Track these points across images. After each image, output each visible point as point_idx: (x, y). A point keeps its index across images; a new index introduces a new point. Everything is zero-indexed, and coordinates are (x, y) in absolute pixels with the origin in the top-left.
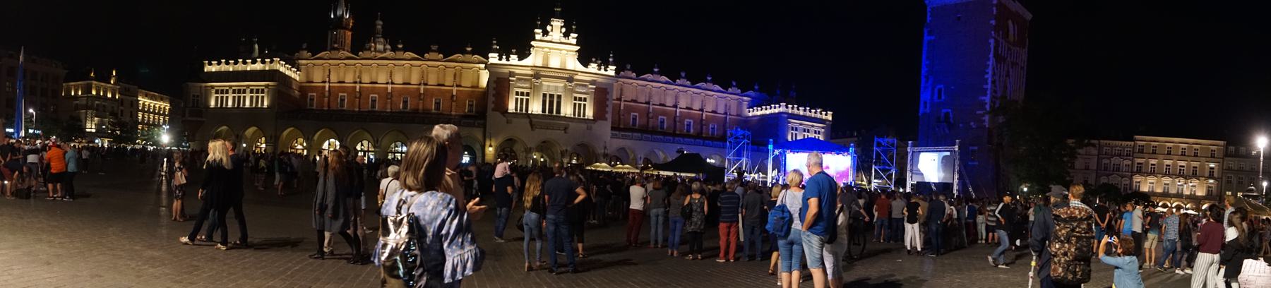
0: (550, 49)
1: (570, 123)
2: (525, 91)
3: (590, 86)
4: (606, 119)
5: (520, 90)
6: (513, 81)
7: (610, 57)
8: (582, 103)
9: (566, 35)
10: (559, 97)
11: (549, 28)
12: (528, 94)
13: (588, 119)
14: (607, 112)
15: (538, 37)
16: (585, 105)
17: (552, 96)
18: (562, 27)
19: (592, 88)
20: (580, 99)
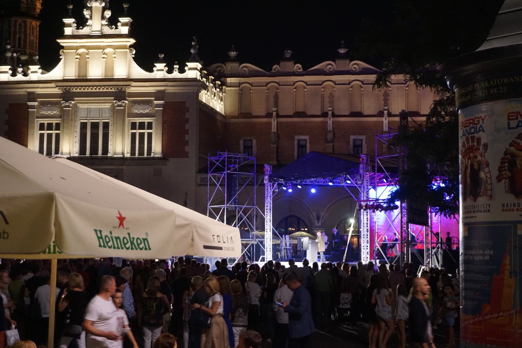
0: (88, 48)
1: (124, 167)
2: (54, 121)
3: (156, 102)
4: (186, 155)
5: (46, 121)
6: (33, 107)
7: (191, 47)
8: (146, 131)
9: (113, 22)
10: (106, 126)
11: (86, 13)
12: (58, 127)
13: (154, 158)
14: (187, 143)
15: (68, 31)
16: (150, 135)
17: (95, 126)
18: (104, 9)
19: (158, 106)
20: (142, 126)
